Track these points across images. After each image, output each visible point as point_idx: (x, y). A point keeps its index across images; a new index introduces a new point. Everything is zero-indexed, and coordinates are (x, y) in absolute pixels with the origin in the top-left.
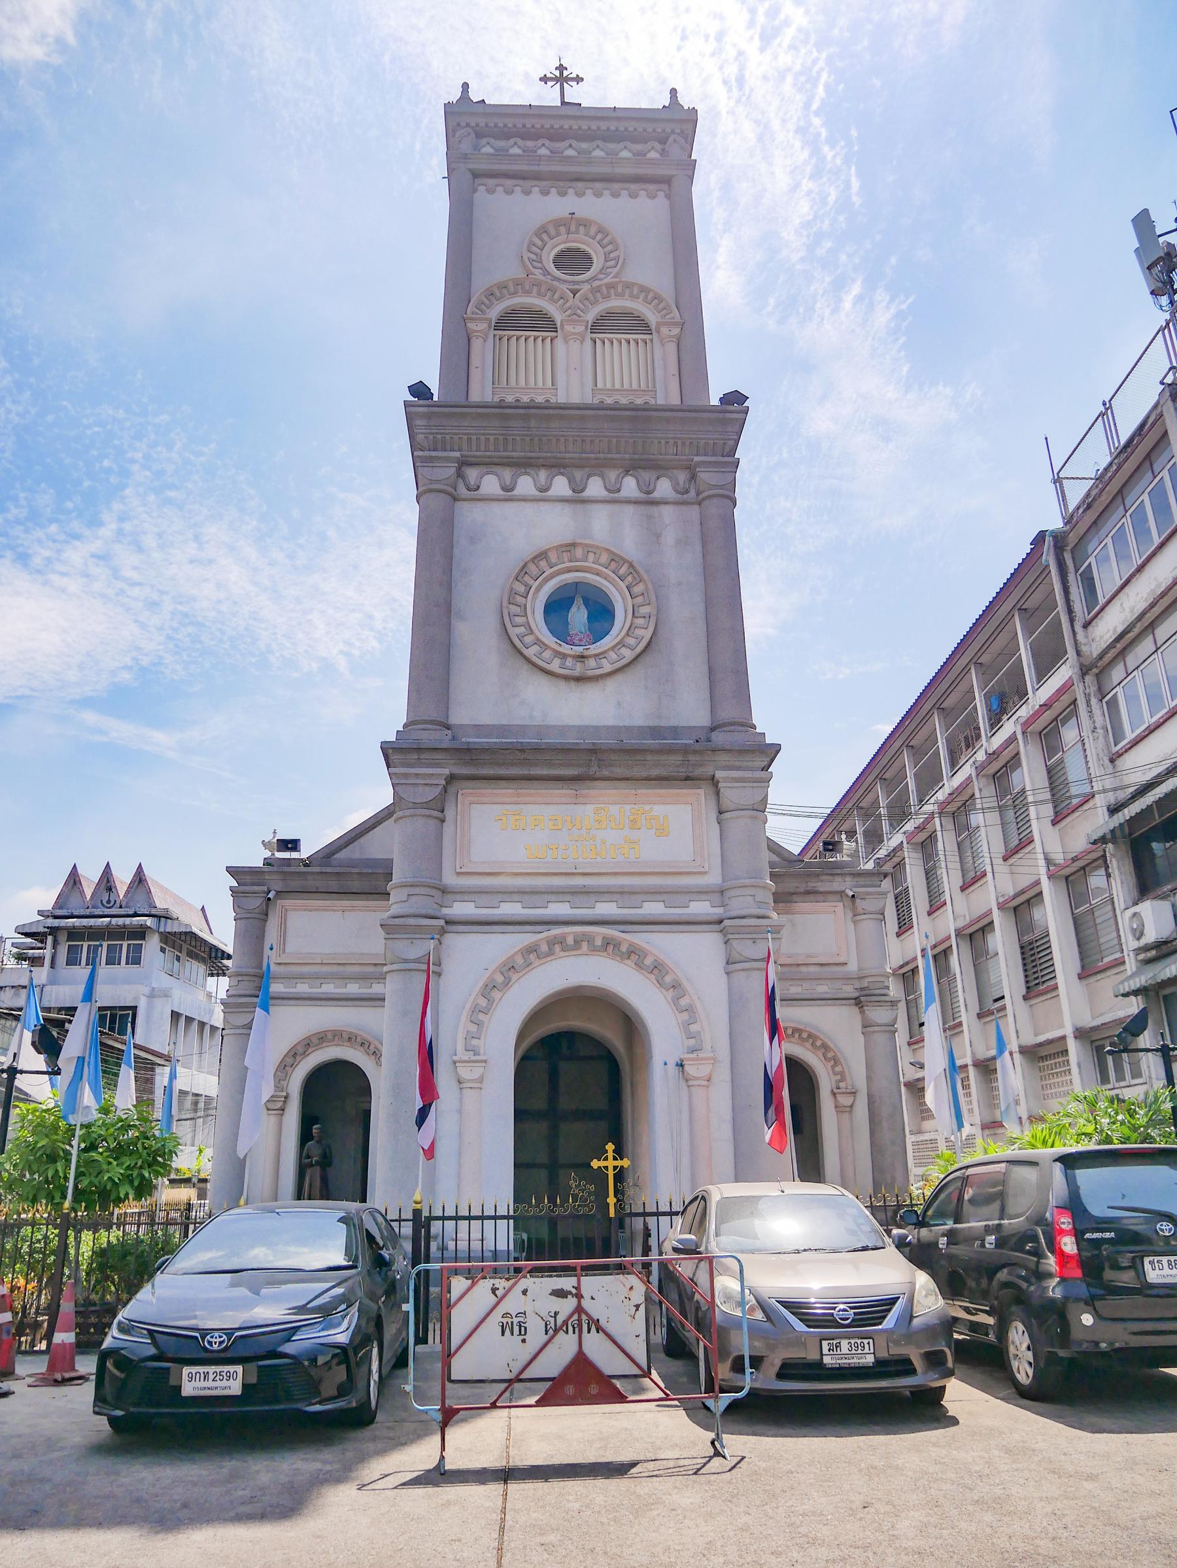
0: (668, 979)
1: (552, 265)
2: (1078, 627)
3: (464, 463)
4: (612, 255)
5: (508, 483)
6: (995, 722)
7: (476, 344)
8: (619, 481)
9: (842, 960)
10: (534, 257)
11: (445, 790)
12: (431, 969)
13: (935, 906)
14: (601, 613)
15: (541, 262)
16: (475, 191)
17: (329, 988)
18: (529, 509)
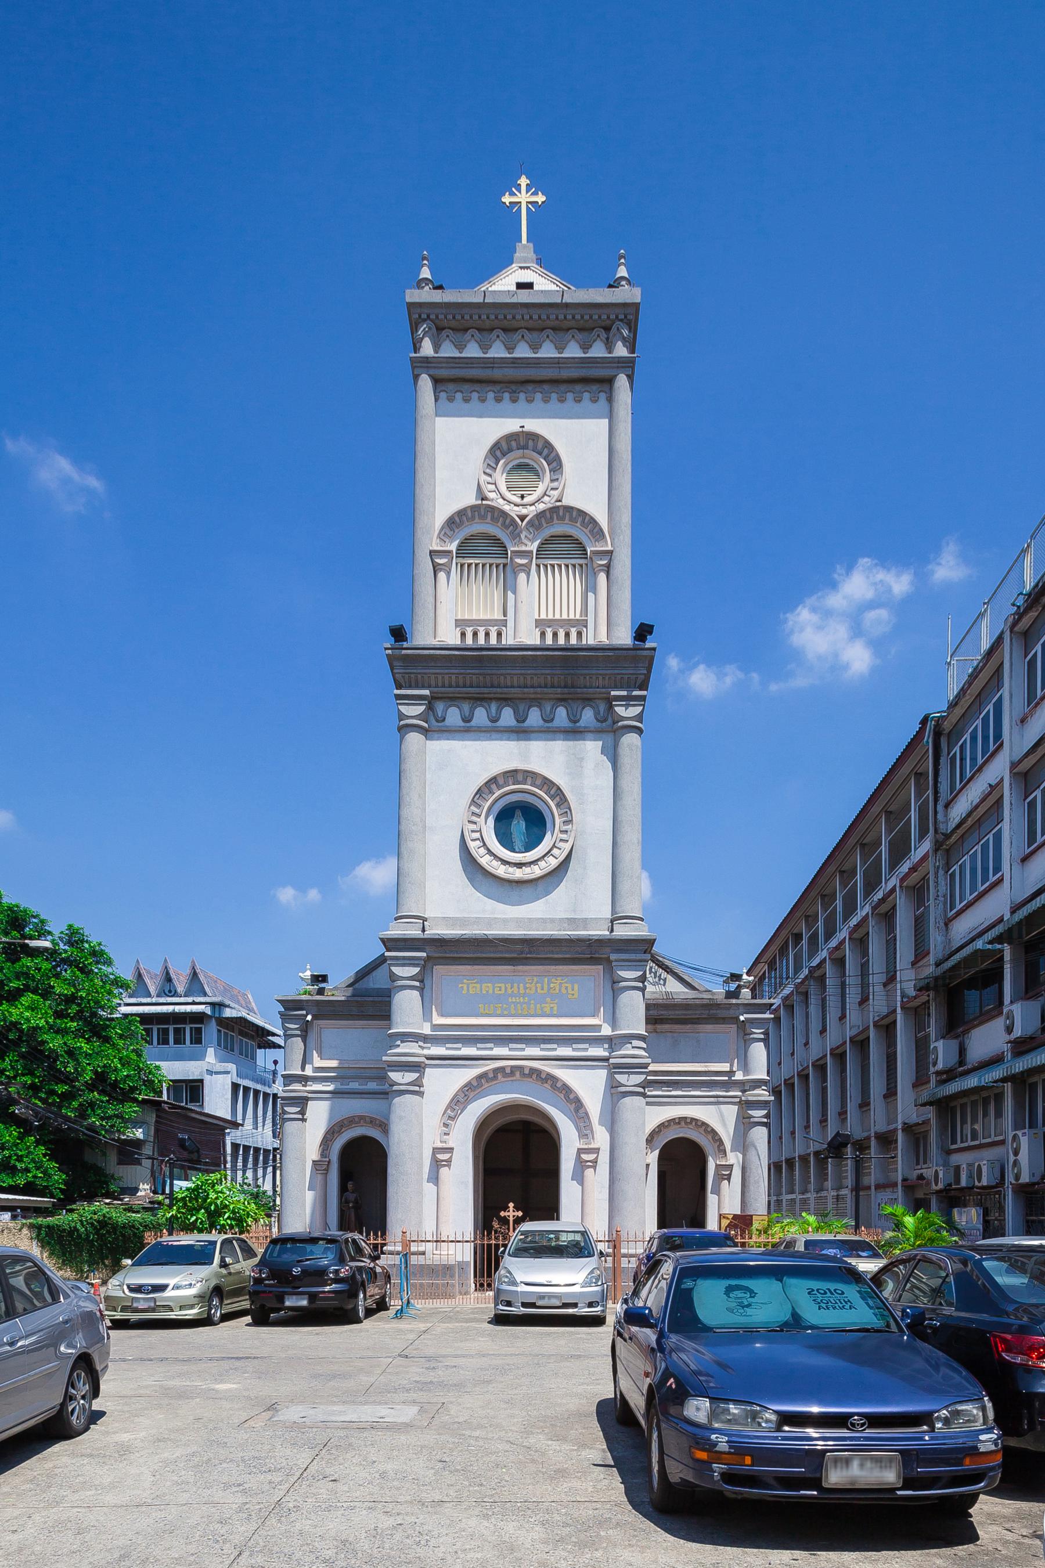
5: (467, 714)
10: (489, 479)
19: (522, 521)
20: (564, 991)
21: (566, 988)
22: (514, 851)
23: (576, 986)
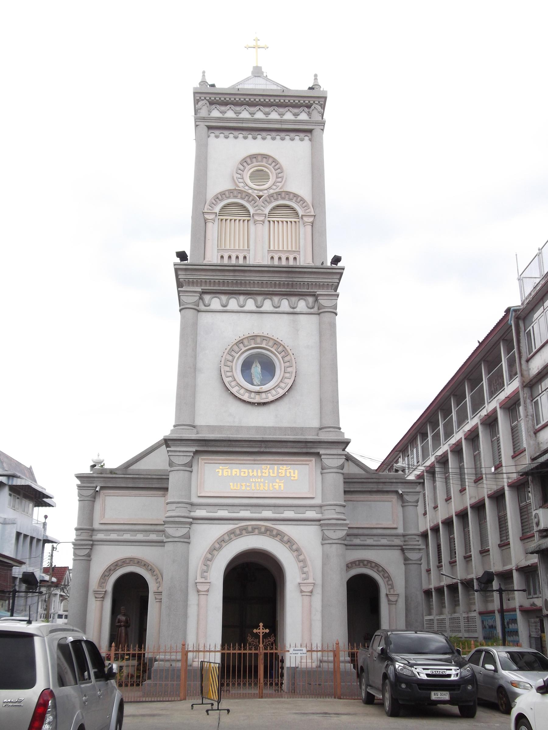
0: (294, 547)
1: (249, 179)
2: (523, 362)
3: (204, 292)
4: (280, 175)
6: (493, 393)
7: (209, 225)
8: (280, 302)
9: (395, 526)
10: (239, 176)
11: (193, 457)
12: (186, 539)
13: (478, 480)
14: (269, 368)
15: (243, 179)
16: (209, 136)
17: (127, 537)
18: (235, 316)
19: (260, 198)
20: (288, 475)
22: (252, 384)
23: (296, 472)
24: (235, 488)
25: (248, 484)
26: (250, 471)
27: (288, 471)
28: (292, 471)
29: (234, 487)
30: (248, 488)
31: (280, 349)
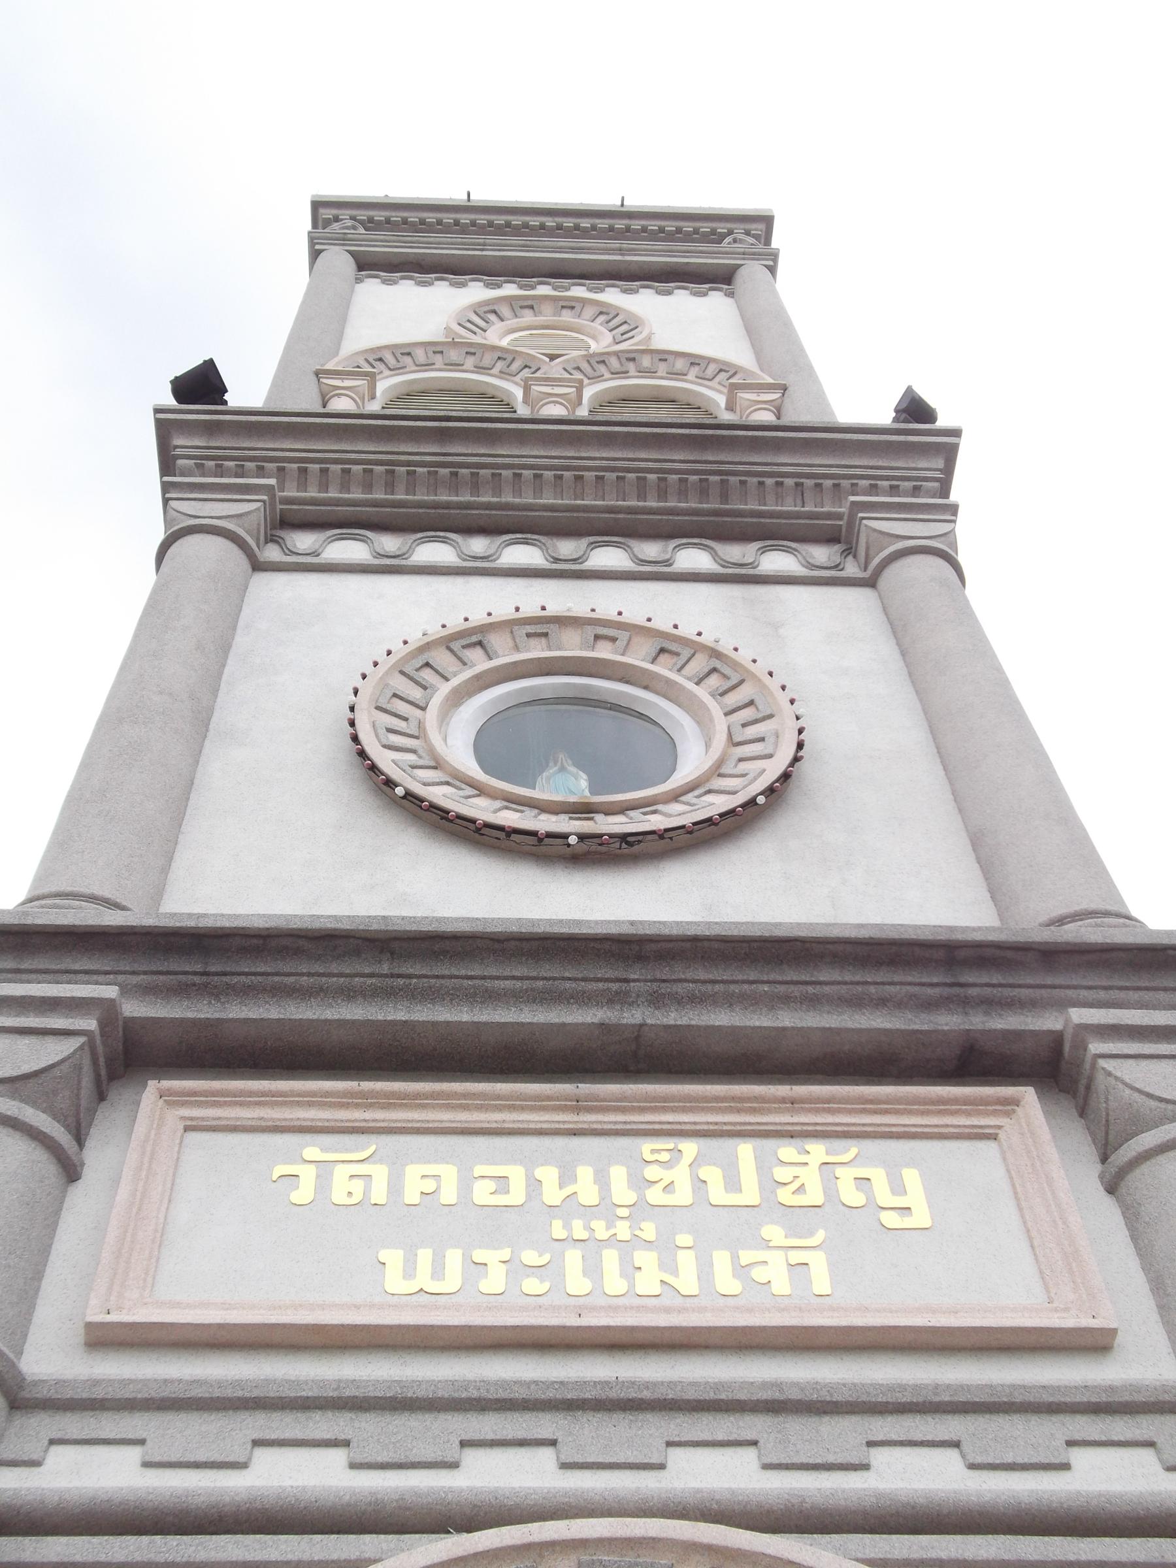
21: (863, 1182)
23: (911, 1177)
24: (423, 1280)
25: (530, 1257)
26: (548, 1175)
27: (845, 1175)
28: (878, 1176)
29: (409, 1272)
30: (532, 1285)
31: (699, 664)
